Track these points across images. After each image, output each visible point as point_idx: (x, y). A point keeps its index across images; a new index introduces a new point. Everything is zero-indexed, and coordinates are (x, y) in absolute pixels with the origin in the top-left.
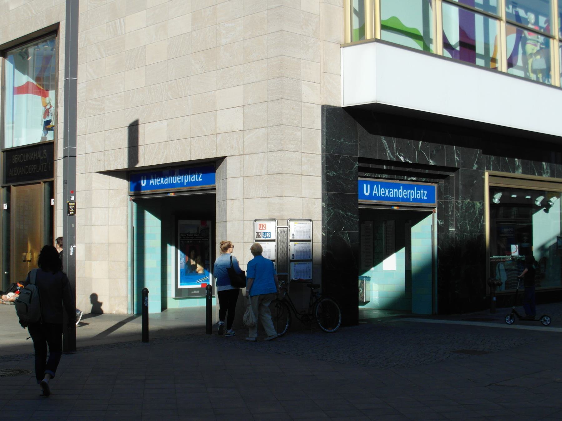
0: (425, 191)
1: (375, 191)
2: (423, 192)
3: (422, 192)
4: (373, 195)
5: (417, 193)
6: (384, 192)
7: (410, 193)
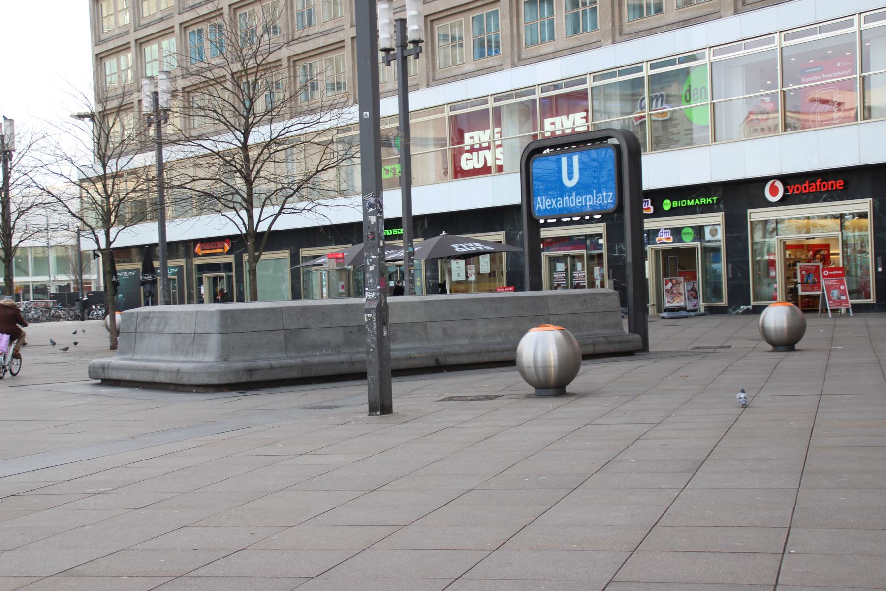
0: (609, 192)
1: (539, 204)
3: (605, 194)
5: (597, 197)
7: (586, 198)
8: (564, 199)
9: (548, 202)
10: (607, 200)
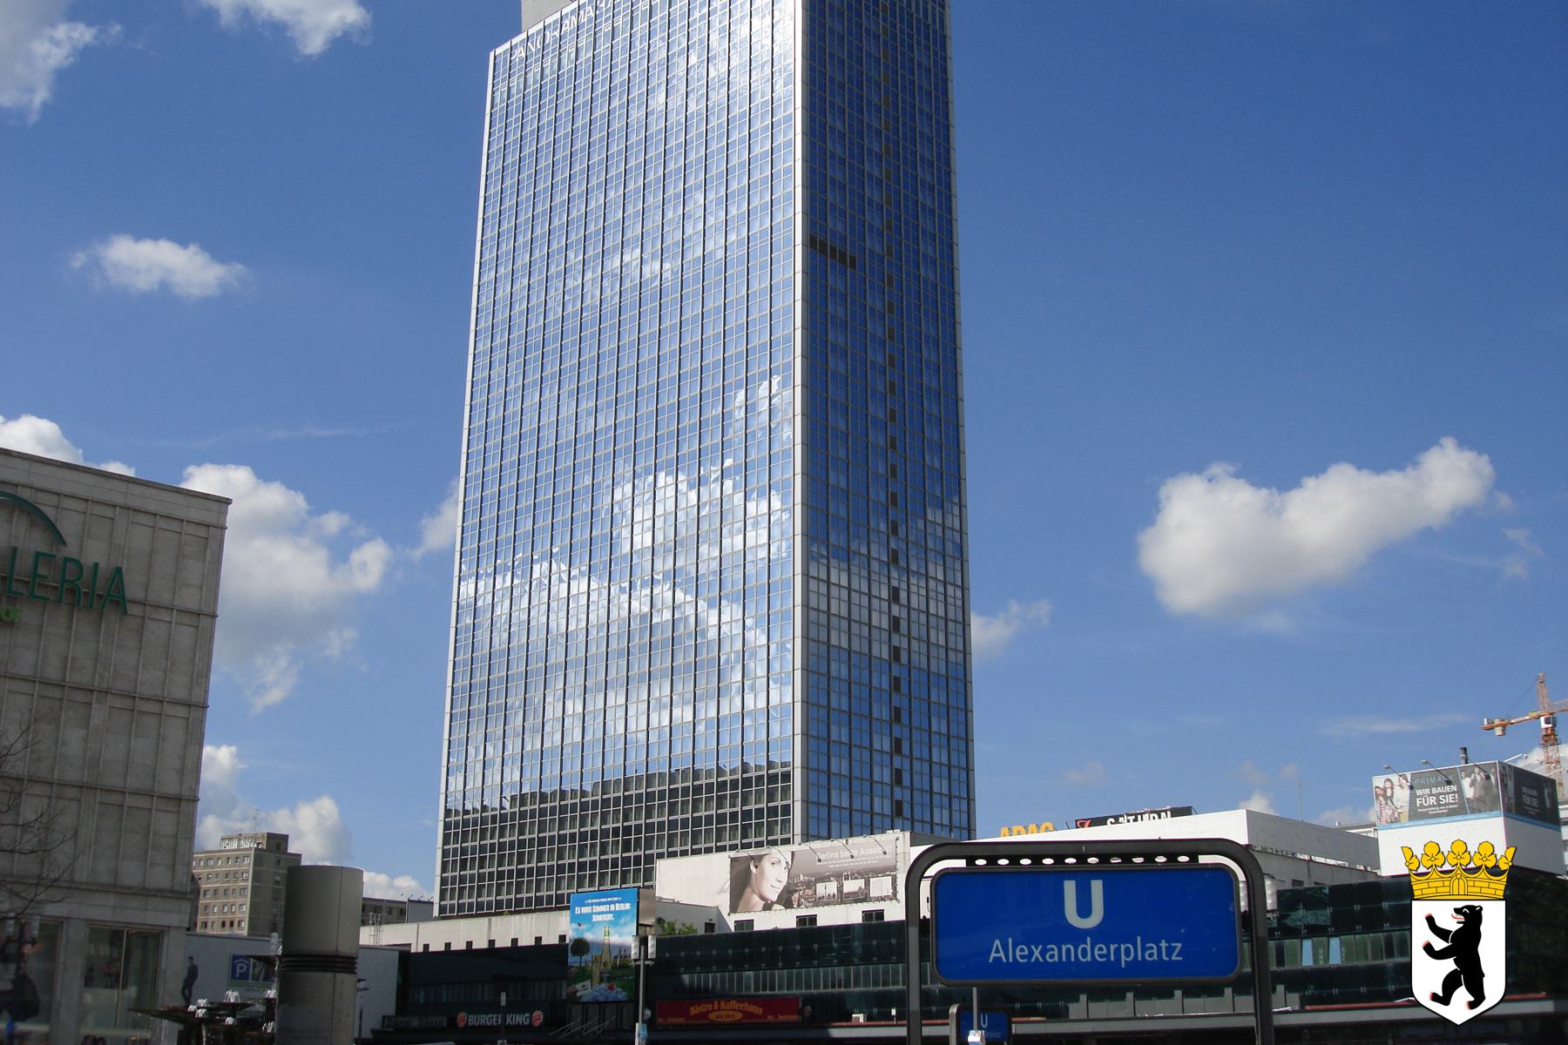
1: (997, 951)
2: (1167, 945)
3: (1164, 944)
4: (991, 961)
6: (1026, 953)
7: (1117, 951)
8: (1064, 948)
9: (1022, 950)
10: (1169, 954)
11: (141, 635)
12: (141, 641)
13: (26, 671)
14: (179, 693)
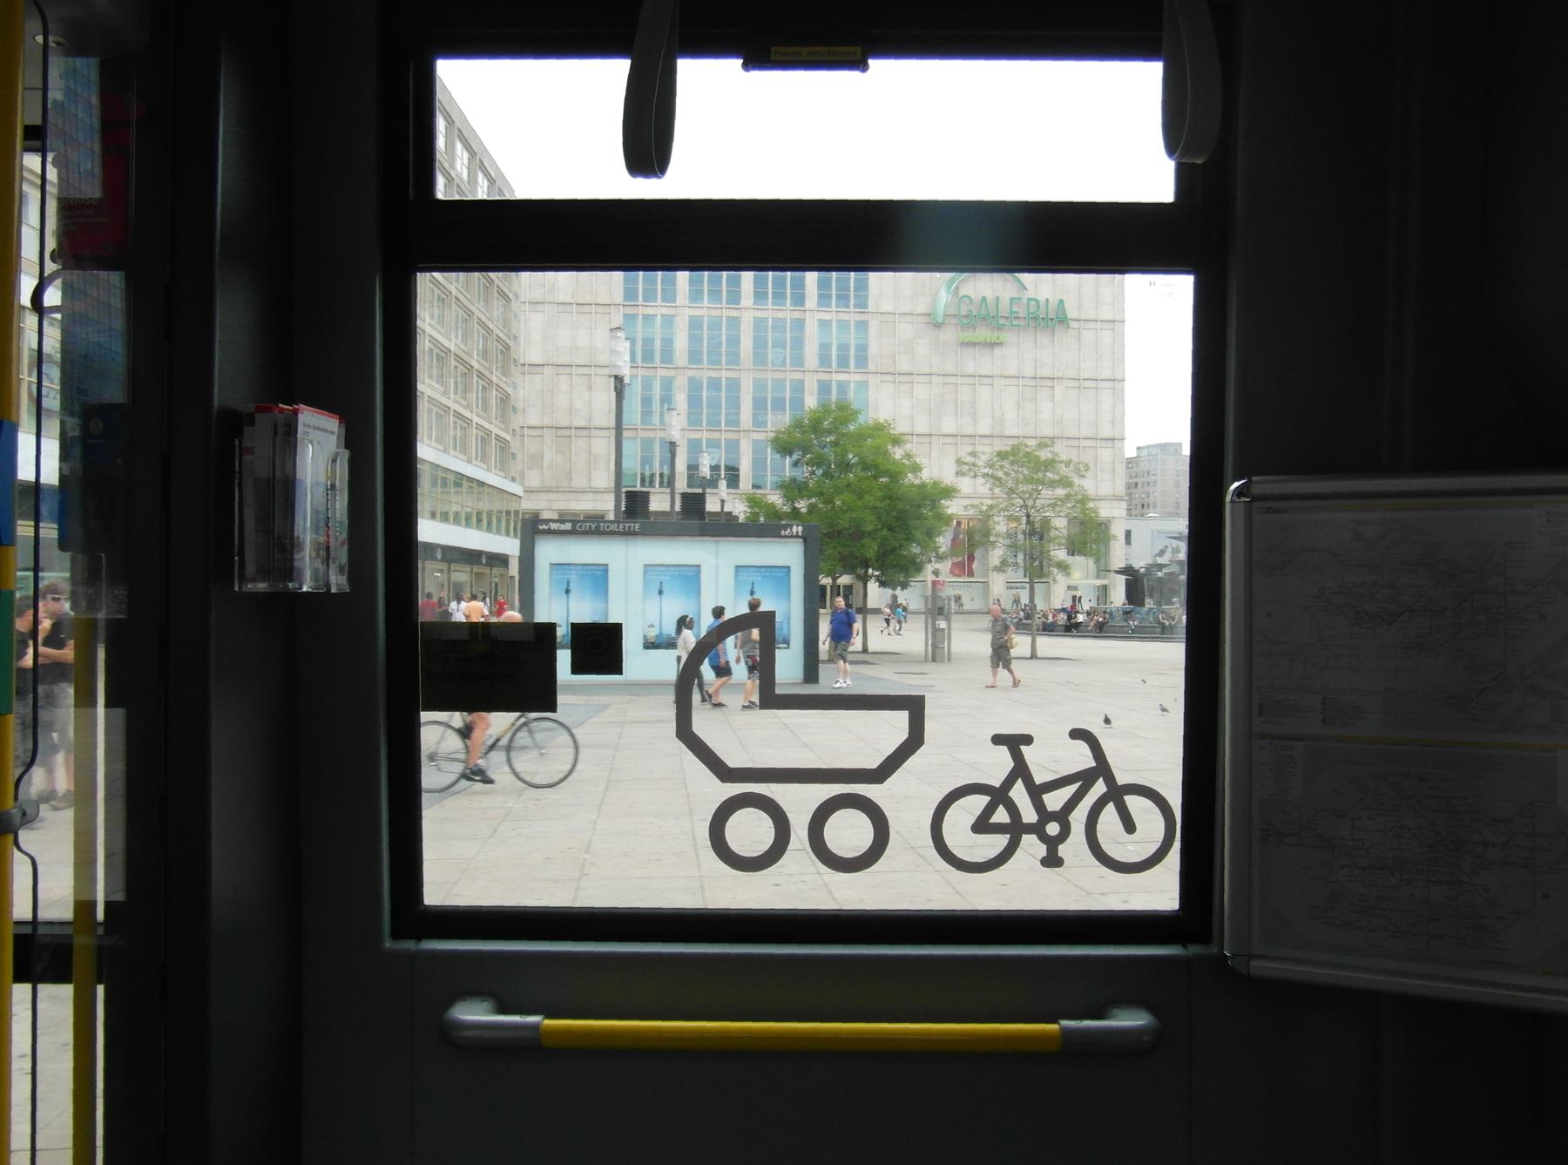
11: (1079, 340)
12: (1080, 343)
13: (1013, 372)
14: (1106, 374)
